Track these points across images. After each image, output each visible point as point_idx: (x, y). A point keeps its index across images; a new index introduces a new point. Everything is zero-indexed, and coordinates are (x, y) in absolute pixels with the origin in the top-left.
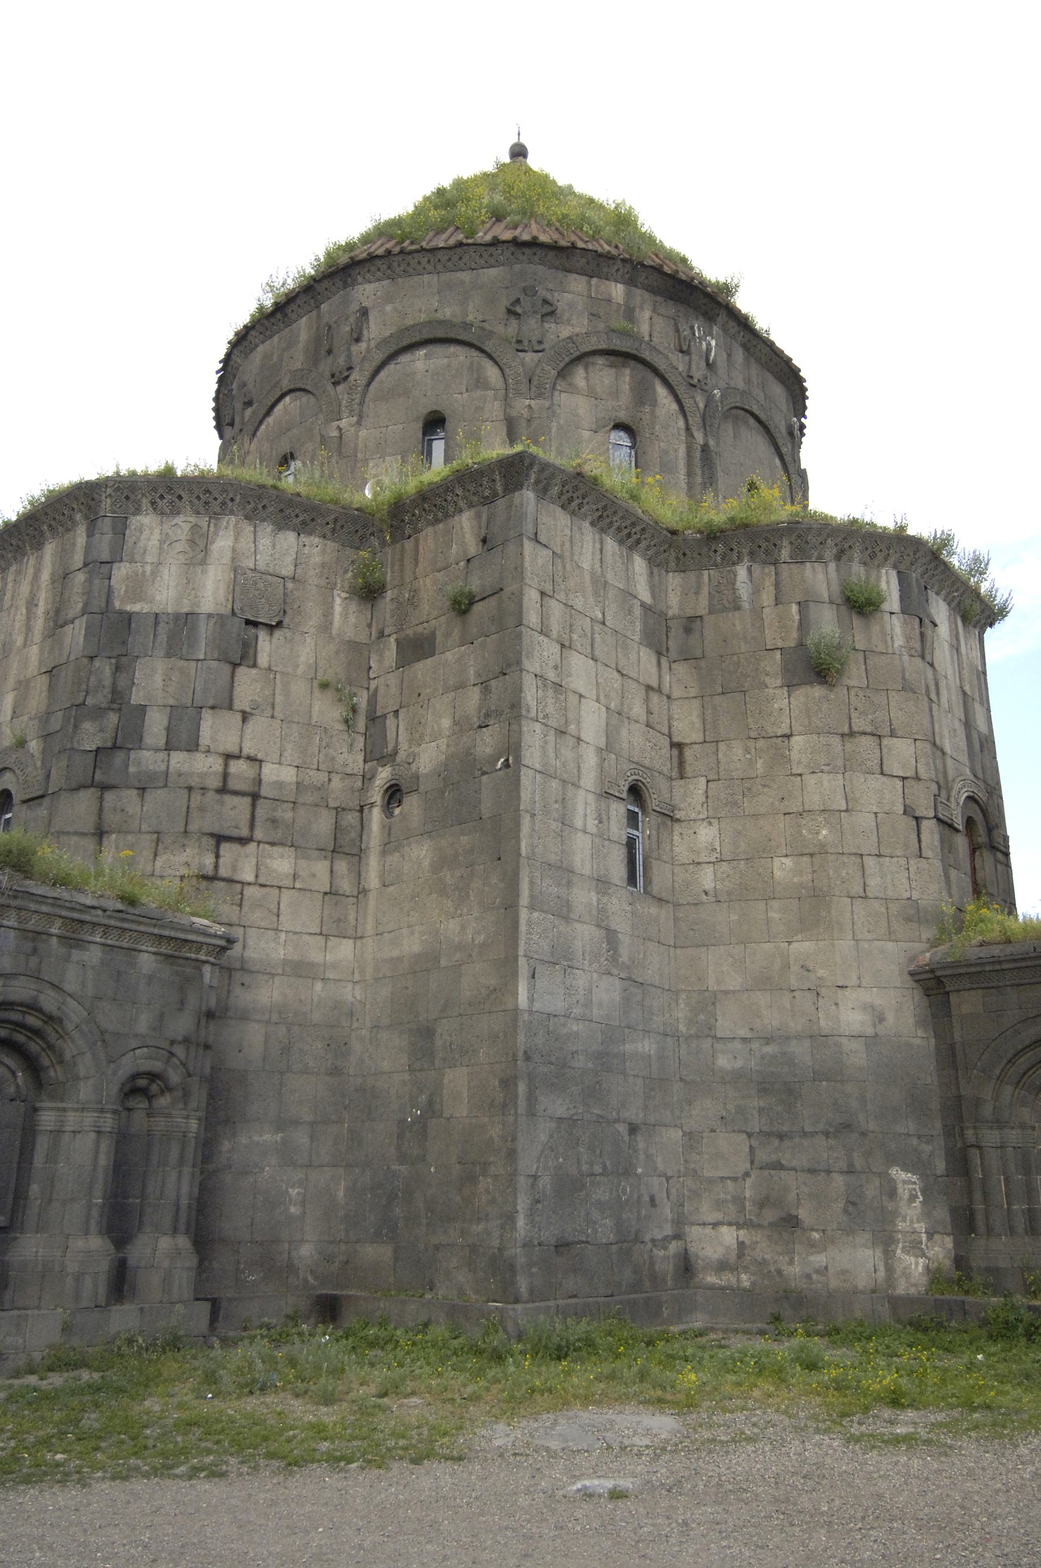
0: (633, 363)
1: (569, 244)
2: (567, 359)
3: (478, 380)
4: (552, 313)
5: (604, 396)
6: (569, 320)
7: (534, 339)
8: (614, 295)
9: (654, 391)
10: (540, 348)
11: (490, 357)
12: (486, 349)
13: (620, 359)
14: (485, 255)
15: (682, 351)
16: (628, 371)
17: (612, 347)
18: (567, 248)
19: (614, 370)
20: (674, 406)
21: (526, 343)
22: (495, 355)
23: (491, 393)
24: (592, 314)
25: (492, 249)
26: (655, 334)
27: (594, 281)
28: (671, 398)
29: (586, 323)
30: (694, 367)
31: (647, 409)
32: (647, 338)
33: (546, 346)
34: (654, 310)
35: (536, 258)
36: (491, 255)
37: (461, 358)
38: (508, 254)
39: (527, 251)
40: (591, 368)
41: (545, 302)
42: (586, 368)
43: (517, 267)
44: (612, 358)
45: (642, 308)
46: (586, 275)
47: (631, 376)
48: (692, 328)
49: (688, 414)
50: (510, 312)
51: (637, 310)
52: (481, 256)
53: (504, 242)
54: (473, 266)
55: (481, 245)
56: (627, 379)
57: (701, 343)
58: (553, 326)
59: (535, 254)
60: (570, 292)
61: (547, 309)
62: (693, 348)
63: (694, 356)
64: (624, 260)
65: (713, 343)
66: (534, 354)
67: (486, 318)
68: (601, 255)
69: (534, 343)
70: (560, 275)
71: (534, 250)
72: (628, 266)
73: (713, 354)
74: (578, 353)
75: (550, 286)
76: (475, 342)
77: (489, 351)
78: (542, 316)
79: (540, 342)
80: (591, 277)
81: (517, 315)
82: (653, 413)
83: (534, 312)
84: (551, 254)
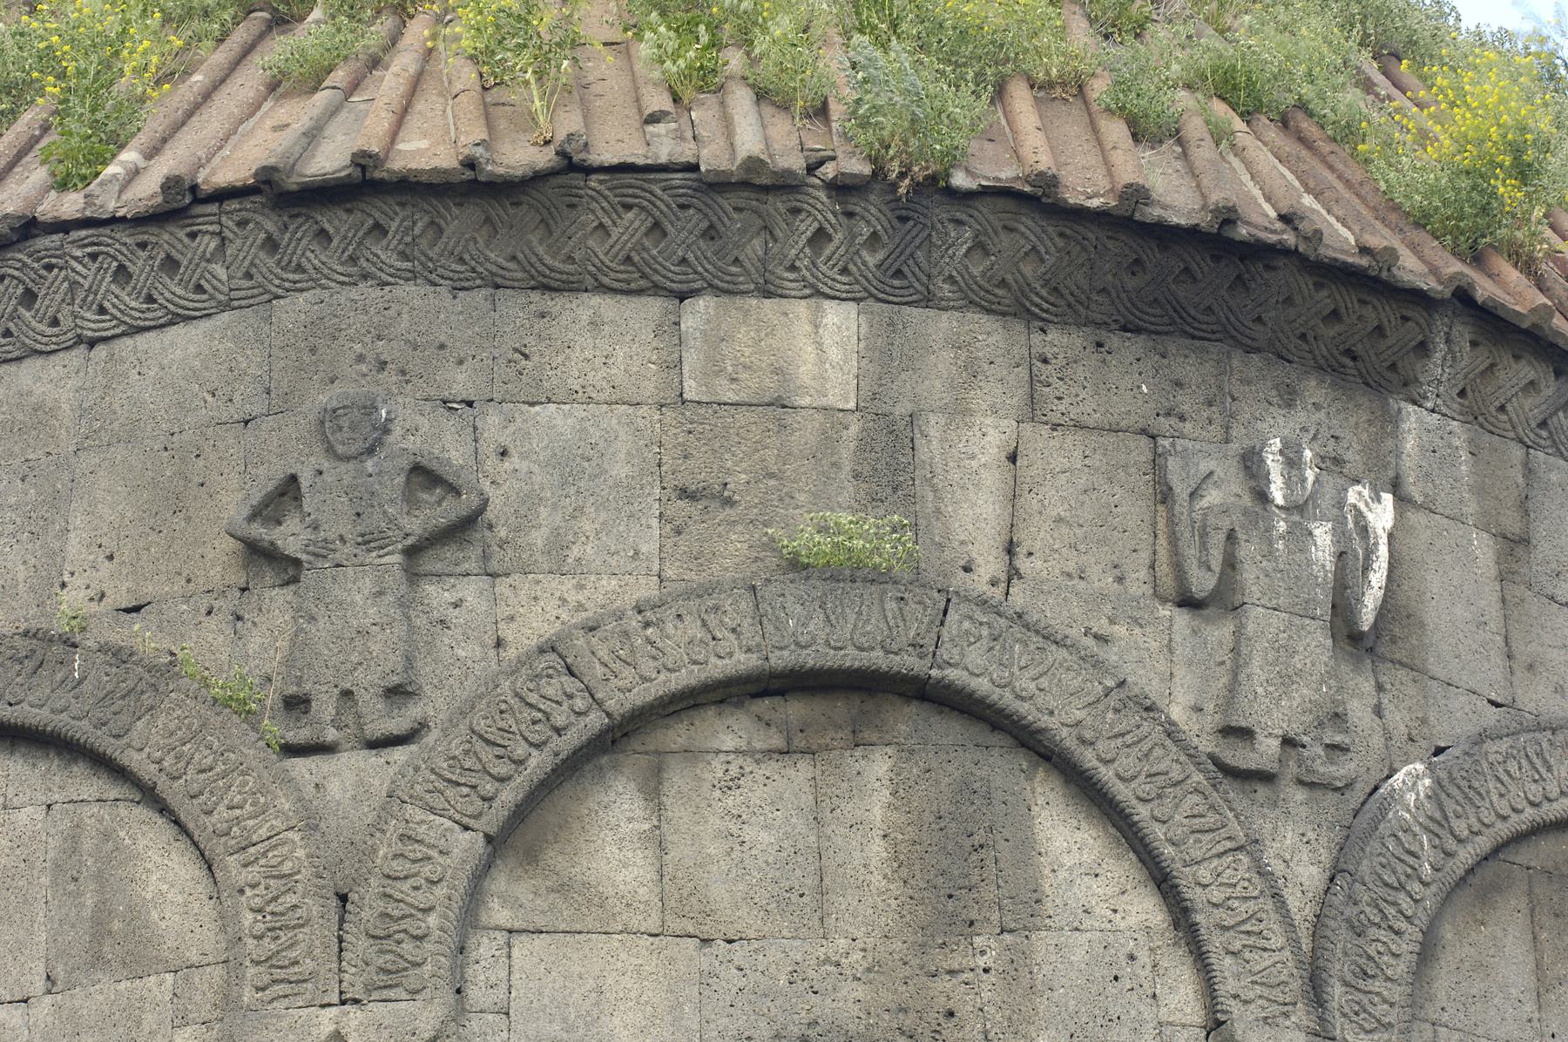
0: (906, 719)
1: (544, 158)
2: (538, 763)
3: (100, 926)
4: (463, 528)
5: (748, 920)
6: (558, 546)
7: (368, 682)
8: (805, 371)
9: (1027, 848)
10: (397, 724)
11: (150, 796)
12: (133, 760)
13: (840, 708)
14: (139, 265)
15: (1188, 602)
16: (878, 766)
17: (782, 659)
18: (538, 178)
19: (802, 771)
20: (1145, 909)
21: (325, 706)
22: (172, 792)
23: (159, 986)
24: (684, 493)
25: (169, 238)
26: (1034, 536)
27: (699, 313)
28: (1122, 869)
29: (649, 547)
30: (1257, 670)
31: (989, 949)
32: (990, 565)
33: (432, 706)
34: (1032, 410)
35: (385, 253)
36: (171, 264)
37: (22, 817)
38: (245, 247)
39: (336, 221)
40: (677, 780)
41: (425, 476)
42: (652, 789)
43: (295, 309)
44: (795, 709)
45: (959, 412)
46: (656, 290)
47: (899, 790)
48: (1251, 464)
49: (1215, 943)
50: (259, 555)
51: (934, 425)
52: (122, 273)
53: (223, 195)
54: (91, 324)
55: (114, 221)
56: (877, 807)
57: (1300, 537)
58: (471, 591)
59: (379, 230)
60: (572, 397)
61: (439, 512)
62: (1250, 576)
63: (1256, 618)
64: (842, 188)
65: (1382, 516)
66: (374, 760)
67: (149, 590)
68: (719, 185)
69: (371, 705)
70: (516, 308)
71: (377, 210)
72: (873, 213)
73: (1378, 578)
74: (596, 721)
75: (461, 382)
76: (83, 730)
77: (148, 772)
78: (412, 552)
79: (397, 693)
80: (682, 297)
81: (288, 568)
82: (1016, 969)
83: (367, 541)
84: (460, 221)
